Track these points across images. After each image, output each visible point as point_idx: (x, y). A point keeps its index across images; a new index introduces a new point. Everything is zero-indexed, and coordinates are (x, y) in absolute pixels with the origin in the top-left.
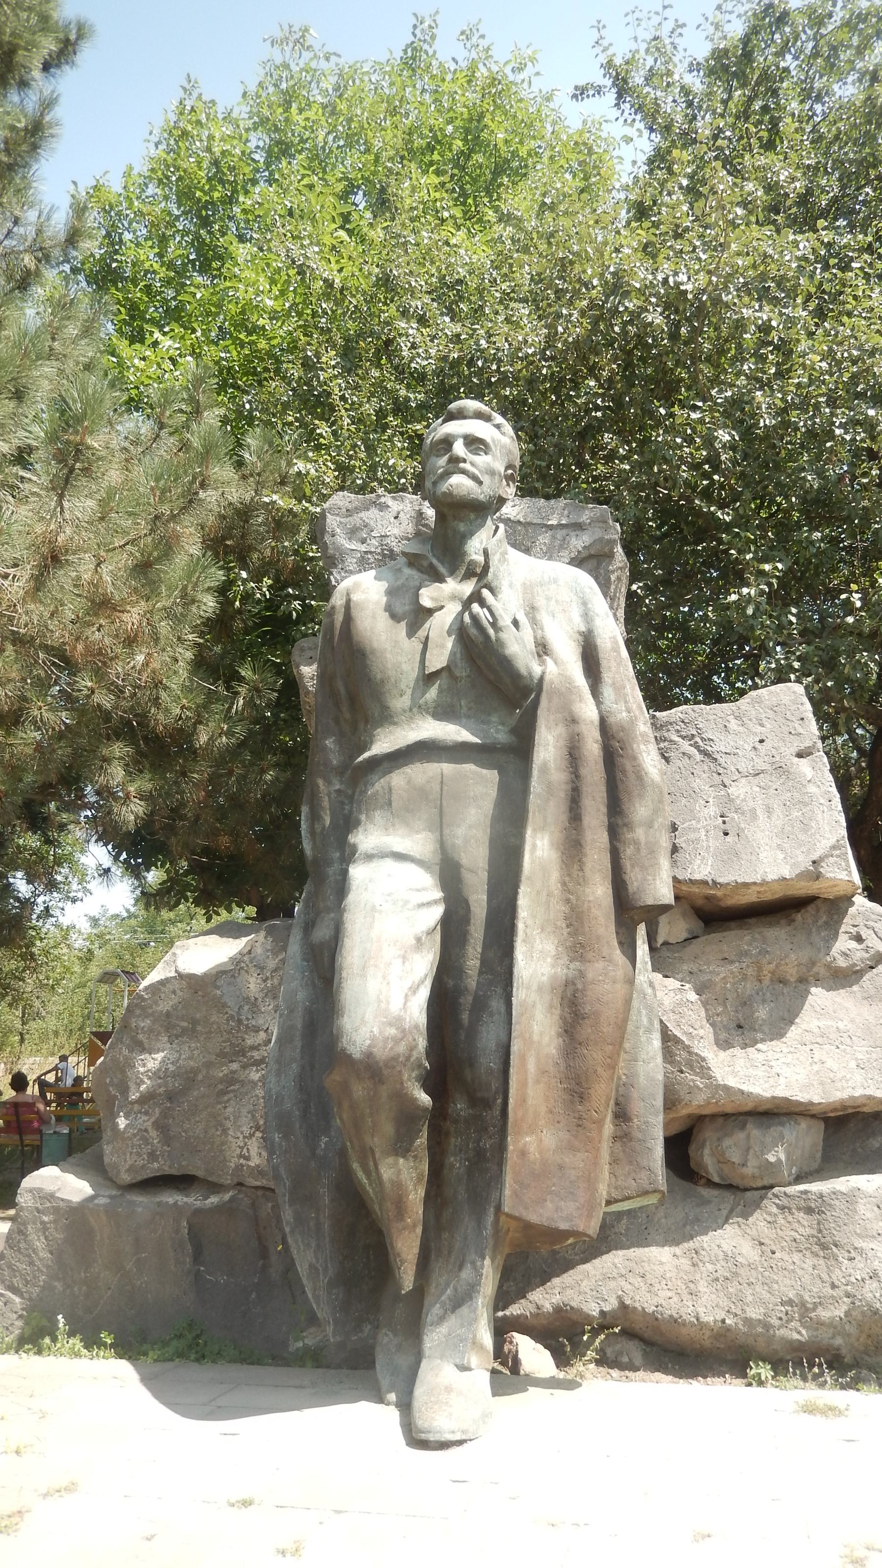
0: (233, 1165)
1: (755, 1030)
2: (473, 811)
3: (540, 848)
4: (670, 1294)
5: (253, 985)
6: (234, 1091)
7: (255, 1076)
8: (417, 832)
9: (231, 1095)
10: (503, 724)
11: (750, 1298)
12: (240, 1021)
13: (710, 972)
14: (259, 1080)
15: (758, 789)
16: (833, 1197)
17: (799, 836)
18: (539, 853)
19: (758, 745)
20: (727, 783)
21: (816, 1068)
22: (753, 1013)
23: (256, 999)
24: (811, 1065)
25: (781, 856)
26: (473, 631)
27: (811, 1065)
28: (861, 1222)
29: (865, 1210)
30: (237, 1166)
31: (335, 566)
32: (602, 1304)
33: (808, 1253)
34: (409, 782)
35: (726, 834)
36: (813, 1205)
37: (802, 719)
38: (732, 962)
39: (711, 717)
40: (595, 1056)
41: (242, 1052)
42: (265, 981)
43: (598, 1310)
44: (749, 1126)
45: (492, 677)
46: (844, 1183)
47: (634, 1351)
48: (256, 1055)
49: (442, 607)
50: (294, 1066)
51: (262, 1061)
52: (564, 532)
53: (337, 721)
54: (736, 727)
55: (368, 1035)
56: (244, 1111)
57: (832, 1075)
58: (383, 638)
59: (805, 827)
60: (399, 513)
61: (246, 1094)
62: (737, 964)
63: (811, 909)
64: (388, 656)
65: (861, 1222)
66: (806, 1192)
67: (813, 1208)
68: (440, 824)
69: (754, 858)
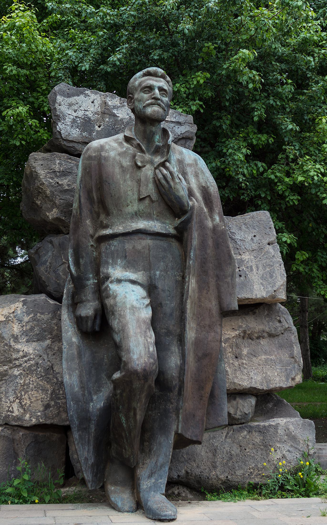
0: (3, 415)
1: (242, 359)
2: (162, 264)
3: (192, 283)
4: (205, 467)
5: (16, 329)
6: (5, 380)
7: (16, 372)
8: (139, 271)
9: (4, 382)
10: (171, 224)
11: (237, 468)
12: (10, 346)
13: (229, 334)
14: (19, 375)
15: (253, 257)
16: (269, 427)
17: (269, 279)
18: (193, 285)
19: (254, 238)
20: (242, 253)
21: (264, 375)
22: (242, 352)
23: (17, 336)
24: (263, 374)
25: (262, 288)
26: (163, 182)
27: (263, 374)
28: (279, 436)
29: (280, 431)
30: (6, 416)
31: (60, 121)
32: (179, 473)
33: (259, 449)
34: (134, 247)
35: (240, 276)
36: (261, 430)
37: (270, 228)
38: (236, 330)
39: (234, 223)
40: (209, 371)
41: (10, 361)
42: (22, 327)
43: (177, 475)
44: (238, 399)
45: (170, 204)
46: (273, 422)
47: (185, 492)
48: (17, 362)
49: (145, 166)
50: (77, 372)
51: (20, 365)
52: (173, 125)
53: (91, 213)
54: (244, 229)
55: (143, 362)
56: (10, 390)
57: (270, 378)
58: (119, 177)
59: (271, 277)
60: (94, 100)
61: (12, 381)
62: (238, 331)
63: (261, 307)
64: (121, 186)
65: (279, 436)
66: (259, 425)
67: (262, 431)
68: (148, 268)
69: (252, 287)
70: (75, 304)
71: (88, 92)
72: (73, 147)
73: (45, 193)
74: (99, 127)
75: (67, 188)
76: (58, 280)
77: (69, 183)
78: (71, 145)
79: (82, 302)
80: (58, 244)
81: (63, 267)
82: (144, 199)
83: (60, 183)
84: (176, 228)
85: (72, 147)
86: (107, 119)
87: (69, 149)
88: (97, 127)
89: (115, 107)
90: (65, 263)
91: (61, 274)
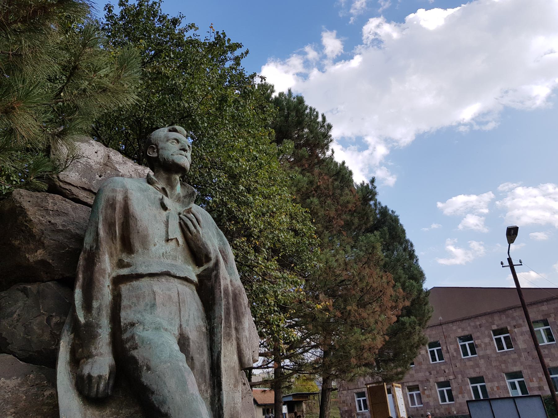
70: (76, 361)
71: (93, 142)
72: (70, 190)
73: (30, 231)
74: (100, 176)
75: (61, 228)
76: (28, 336)
77: (64, 223)
78: (67, 187)
79: (90, 356)
80: (35, 292)
81: (39, 319)
82: (172, 240)
83: (52, 221)
84: (198, 276)
85: (67, 190)
86: (109, 172)
87: (64, 191)
88: (97, 176)
89: (117, 163)
90: (44, 314)
91: (35, 328)
